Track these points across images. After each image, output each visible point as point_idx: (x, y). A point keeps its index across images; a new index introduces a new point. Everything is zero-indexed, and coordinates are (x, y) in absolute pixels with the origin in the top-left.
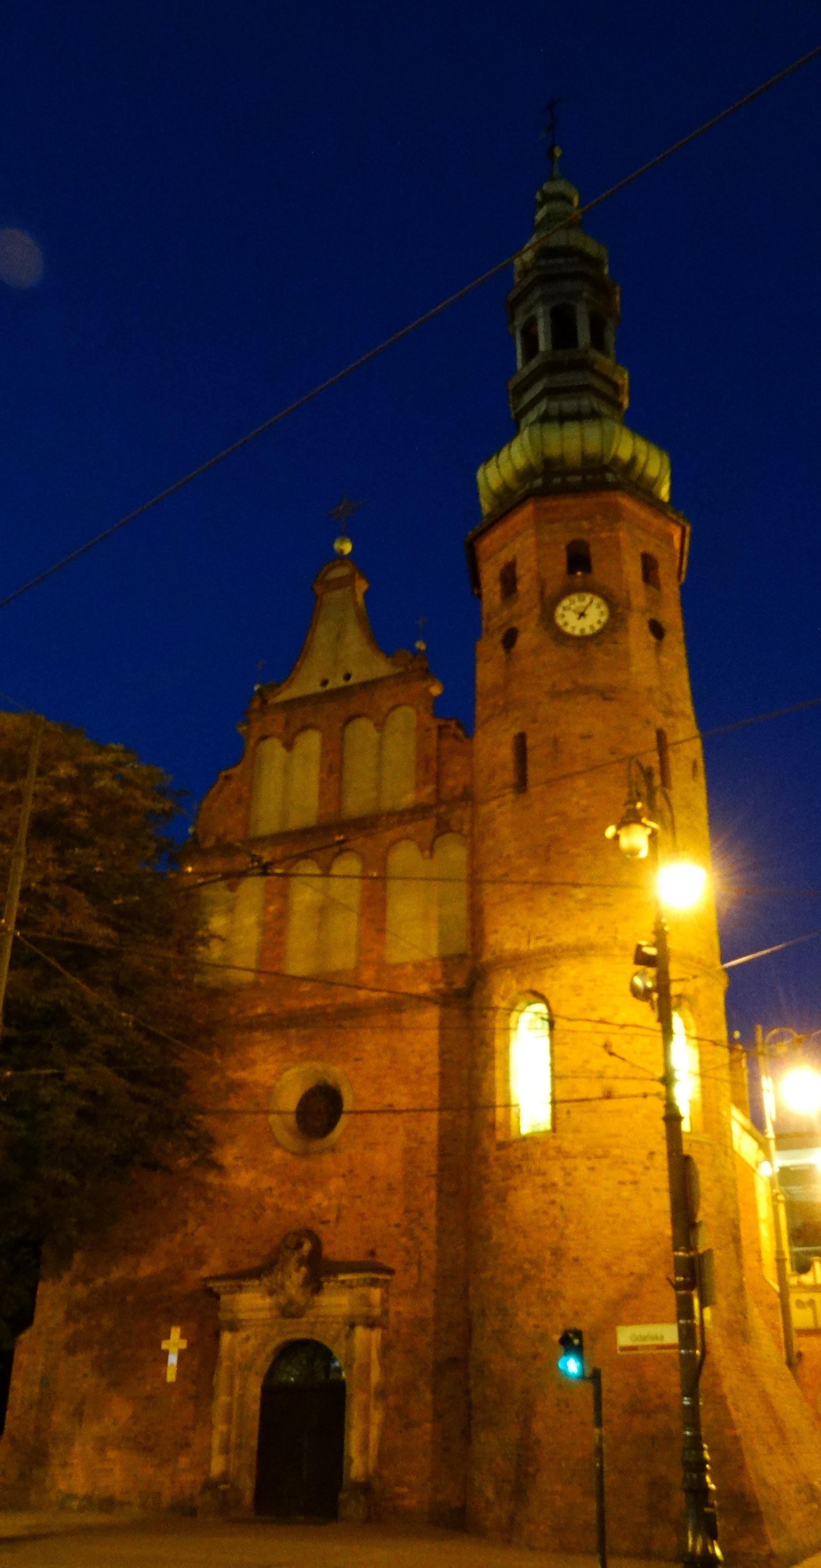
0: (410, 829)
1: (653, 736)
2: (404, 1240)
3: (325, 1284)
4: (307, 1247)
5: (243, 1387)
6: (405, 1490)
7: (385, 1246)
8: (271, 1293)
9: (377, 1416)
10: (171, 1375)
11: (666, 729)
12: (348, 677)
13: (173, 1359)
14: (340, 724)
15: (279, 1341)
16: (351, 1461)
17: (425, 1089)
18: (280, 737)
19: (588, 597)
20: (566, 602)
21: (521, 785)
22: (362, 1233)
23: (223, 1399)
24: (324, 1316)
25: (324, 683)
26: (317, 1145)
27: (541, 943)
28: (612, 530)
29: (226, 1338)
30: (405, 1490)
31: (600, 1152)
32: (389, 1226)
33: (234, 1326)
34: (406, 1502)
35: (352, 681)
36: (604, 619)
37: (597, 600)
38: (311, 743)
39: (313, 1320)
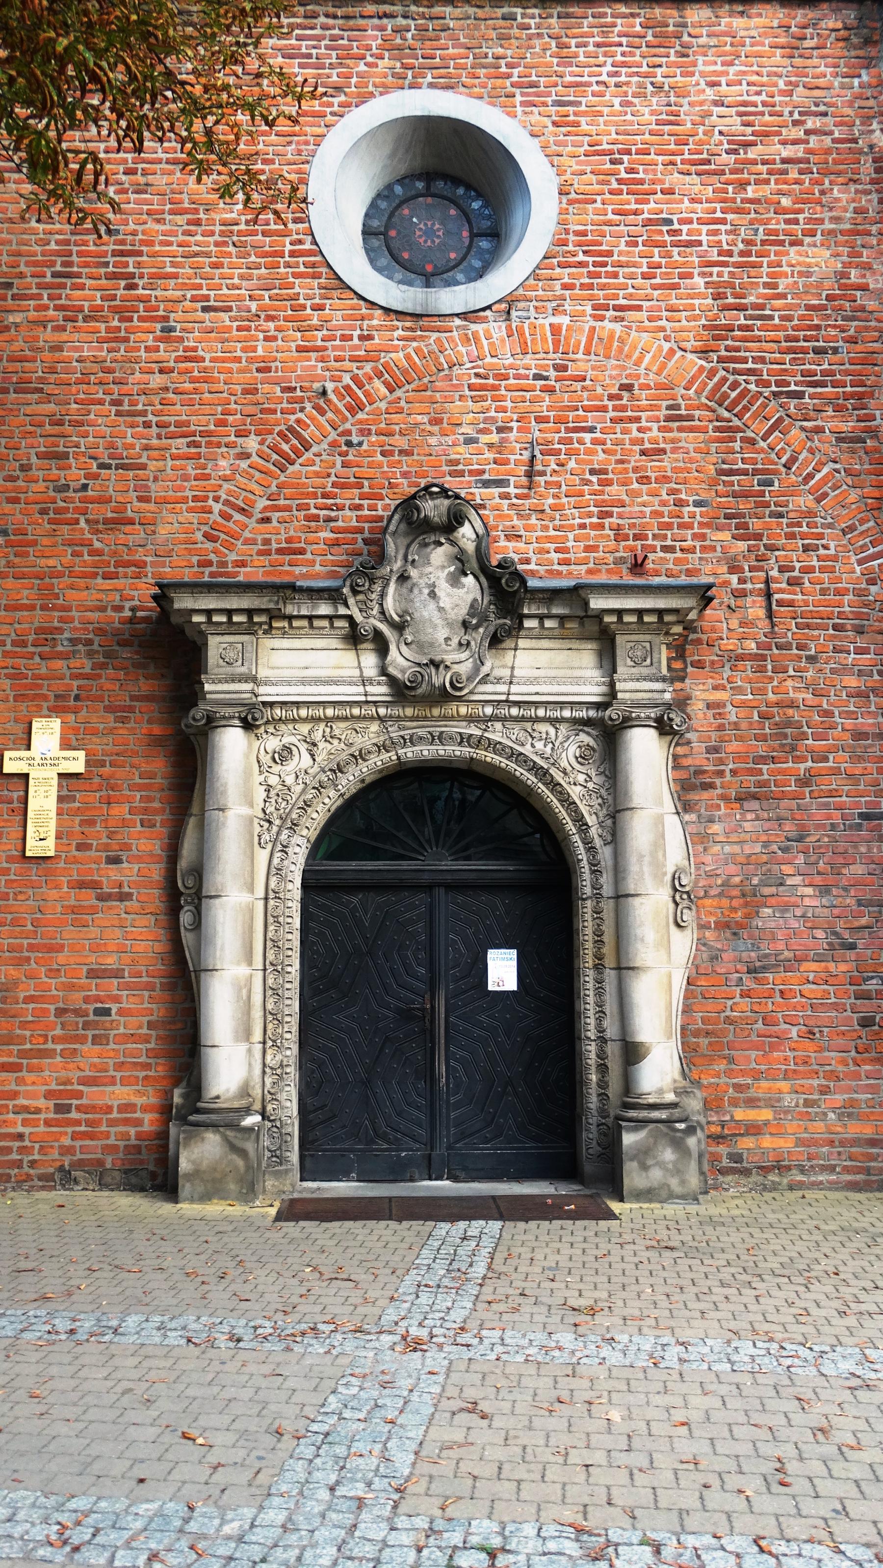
2: (726, 536)
3: (528, 624)
4: (466, 534)
5: (274, 871)
6: (766, 1114)
7: (665, 549)
9: (683, 944)
13: (43, 802)
15: (378, 761)
16: (632, 1053)
17: (766, 191)
22: (603, 515)
24: (518, 704)
26: (452, 298)
30: (766, 1114)
32: (680, 503)
34: (767, 1142)
39: (489, 710)
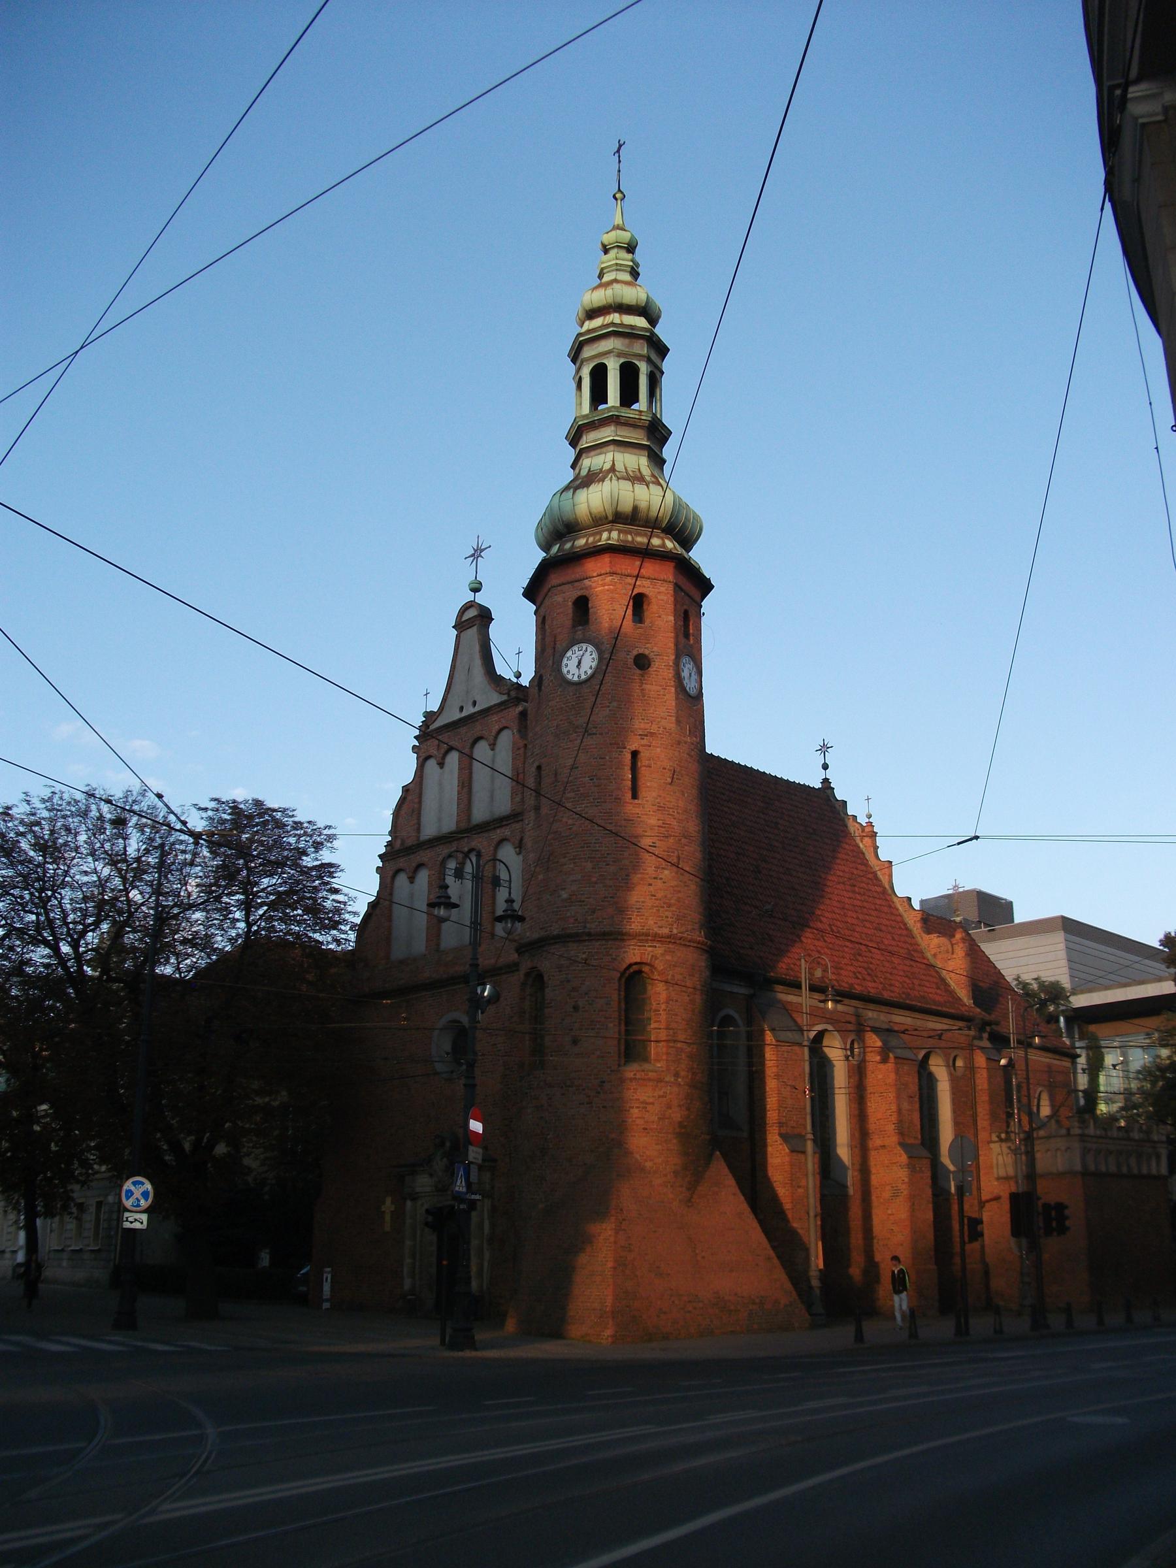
0: (506, 832)
1: (629, 756)
4: (448, 1144)
8: (431, 1175)
9: (487, 1255)
10: (387, 1228)
11: (641, 749)
12: (474, 703)
13: (388, 1218)
14: (469, 745)
18: (435, 757)
19: (584, 646)
20: (569, 653)
21: (537, 808)
23: (408, 1243)
25: (461, 709)
27: (543, 933)
28: (604, 585)
29: (409, 1203)
31: (568, 1083)
33: (414, 1198)
35: (477, 709)
36: (594, 664)
37: (590, 648)
38: (453, 758)
